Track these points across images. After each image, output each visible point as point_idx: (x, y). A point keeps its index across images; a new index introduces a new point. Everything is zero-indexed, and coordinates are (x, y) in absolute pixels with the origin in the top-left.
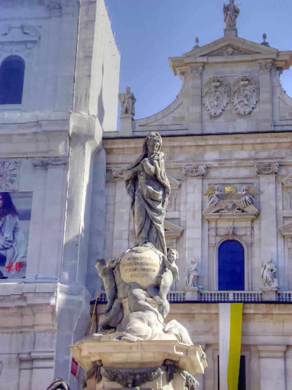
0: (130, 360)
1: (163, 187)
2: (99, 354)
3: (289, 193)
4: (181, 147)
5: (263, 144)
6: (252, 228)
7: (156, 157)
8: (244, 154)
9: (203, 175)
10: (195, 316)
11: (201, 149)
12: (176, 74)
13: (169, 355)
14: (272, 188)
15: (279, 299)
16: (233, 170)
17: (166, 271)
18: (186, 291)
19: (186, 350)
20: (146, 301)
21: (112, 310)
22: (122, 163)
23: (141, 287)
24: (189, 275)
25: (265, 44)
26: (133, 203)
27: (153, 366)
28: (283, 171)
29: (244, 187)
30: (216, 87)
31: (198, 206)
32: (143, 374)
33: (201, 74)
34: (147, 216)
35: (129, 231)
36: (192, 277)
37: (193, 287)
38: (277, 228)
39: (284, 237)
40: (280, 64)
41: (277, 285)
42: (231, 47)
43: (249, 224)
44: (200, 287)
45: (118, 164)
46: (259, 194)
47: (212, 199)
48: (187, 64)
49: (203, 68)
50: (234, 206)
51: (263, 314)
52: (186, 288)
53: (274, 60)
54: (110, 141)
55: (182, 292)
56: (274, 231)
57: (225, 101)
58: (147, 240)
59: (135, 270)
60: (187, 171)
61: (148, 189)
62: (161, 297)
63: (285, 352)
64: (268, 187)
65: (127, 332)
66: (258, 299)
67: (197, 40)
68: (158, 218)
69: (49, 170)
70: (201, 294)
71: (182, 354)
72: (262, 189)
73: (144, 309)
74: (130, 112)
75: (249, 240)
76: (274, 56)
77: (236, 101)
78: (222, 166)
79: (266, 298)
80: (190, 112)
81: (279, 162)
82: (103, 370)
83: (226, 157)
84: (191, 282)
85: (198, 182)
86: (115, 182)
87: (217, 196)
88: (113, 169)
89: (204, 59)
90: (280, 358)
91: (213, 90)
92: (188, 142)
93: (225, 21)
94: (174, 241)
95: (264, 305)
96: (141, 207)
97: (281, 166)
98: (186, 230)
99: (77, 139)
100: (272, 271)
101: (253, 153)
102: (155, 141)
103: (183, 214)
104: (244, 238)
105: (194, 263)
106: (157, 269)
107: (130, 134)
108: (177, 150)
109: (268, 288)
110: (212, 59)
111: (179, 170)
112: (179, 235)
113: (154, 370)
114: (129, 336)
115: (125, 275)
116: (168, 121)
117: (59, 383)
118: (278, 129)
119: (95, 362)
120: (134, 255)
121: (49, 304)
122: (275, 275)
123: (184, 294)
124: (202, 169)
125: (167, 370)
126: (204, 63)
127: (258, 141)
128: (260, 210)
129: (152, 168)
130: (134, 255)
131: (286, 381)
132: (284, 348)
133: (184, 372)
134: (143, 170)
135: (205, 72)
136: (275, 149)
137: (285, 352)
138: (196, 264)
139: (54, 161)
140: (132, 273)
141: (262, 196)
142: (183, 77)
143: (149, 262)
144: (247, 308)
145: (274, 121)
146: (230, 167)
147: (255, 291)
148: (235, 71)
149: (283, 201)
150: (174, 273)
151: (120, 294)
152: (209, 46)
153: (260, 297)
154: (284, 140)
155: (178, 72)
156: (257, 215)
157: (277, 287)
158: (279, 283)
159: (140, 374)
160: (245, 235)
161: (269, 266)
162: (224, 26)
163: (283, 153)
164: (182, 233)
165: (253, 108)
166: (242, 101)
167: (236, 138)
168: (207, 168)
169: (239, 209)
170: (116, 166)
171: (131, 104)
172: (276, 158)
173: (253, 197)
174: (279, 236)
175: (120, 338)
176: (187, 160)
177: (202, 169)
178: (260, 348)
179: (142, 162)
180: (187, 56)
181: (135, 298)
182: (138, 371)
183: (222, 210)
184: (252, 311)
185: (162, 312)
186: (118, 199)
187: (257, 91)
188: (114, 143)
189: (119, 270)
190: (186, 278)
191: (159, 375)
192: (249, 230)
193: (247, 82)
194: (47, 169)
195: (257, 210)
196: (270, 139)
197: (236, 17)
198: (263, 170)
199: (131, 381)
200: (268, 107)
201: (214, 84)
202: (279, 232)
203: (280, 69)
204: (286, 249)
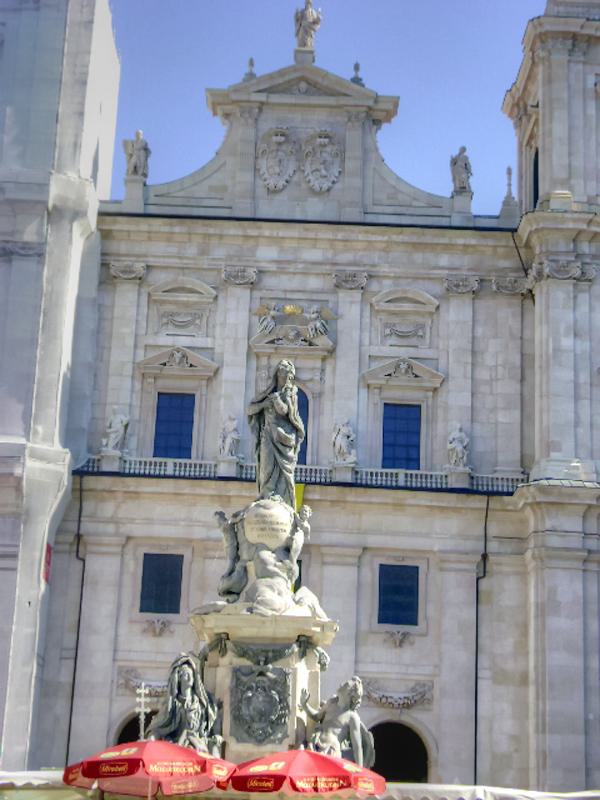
0: (261, 635)
1: (295, 429)
2: (227, 627)
3: (381, 320)
4: (221, 236)
5: (347, 241)
6: (323, 370)
7: (289, 393)
8: (315, 255)
9: (252, 283)
10: (232, 499)
11: (251, 242)
12: (215, 114)
13: (304, 630)
14: (355, 310)
15: (356, 479)
16: (298, 277)
17: (297, 531)
18: (219, 462)
19: (323, 626)
20: (275, 565)
21: (235, 573)
22: (127, 255)
23: (269, 549)
24: (225, 438)
25: (357, 80)
26: (258, 444)
27: (287, 642)
28: (374, 286)
29: (315, 307)
30: (280, 144)
31: (242, 332)
32: (277, 651)
33: (256, 120)
34: (276, 464)
35: (134, 363)
36: (229, 441)
37: (230, 457)
38: (359, 372)
40: (378, 115)
41: (355, 459)
42: (303, 82)
43: (318, 364)
44: (241, 455)
45: (119, 255)
46: (337, 319)
47: (265, 323)
48: (234, 102)
49: (260, 110)
50: (298, 335)
51: (332, 501)
52: (220, 458)
53: (370, 108)
54: (108, 218)
55: (213, 463)
56: (355, 376)
57: (292, 166)
58: (276, 491)
59: (262, 529)
60: (229, 276)
61: (279, 433)
62: (292, 561)
63: (360, 557)
64: (350, 309)
65: (258, 603)
66: (325, 478)
67: (251, 63)
68: (288, 466)
69: (14, 263)
70: (242, 467)
71: (318, 629)
72: (340, 311)
73: (272, 575)
74: (140, 172)
75: (317, 388)
76: (371, 103)
77: (308, 169)
78: (282, 271)
79: (338, 477)
80: (236, 187)
81: (367, 271)
82: (229, 644)
83: (289, 257)
86: (114, 285)
87: (273, 317)
88: (112, 263)
89: (262, 97)
90: (352, 565)
91: (274, 147)
92: (232, 229)
93: (297, 35)
94: (204, 383)
95: (335, 488)
96: (270, 453)
97: (370, 277)
98: (222, 366)
99: (59, 215)
100: (348, 437)
101: (330, 254)
102: (288, 372)
103: (219, 341)
104: (310, 385)
105: (234, 419)
106: (289, 528)
107: (141, 210)
108: (214, 241)
109: (340, 462)
110: (275, 98)
111: (215, 273)
112: (212, 374)
113: (289, 646)
114: (262, 609)
115: (251, 534)
116: (201, 191)
117: (184, 659)
118: (370, 219)
119: (219, 634)
120: (262, 510)
121: (12, 474)
122: (352, 444)
123: (216, 466)
124: (251, 273)
125: (300, 646)
126: (262, 103)
128: (335, 343)
129: (285, 407)
130: (262, 510)
131: (358, 599)
132: (359, 551)
133: (319, 648)
134: (273, 406)
135: (263, 116)
136: (365, 250)
137: (360, 557)
138: (235, 423)
139: (23, 248)
140: (260, 532)
141: (339, 321)
142: (226, 121)
143: (280, 521)
144: (309, 492)
145: (364, 206)
146: (294, 274)
147: (321, 465)
148: (311, 120)
149: (370, 332)
150: (306, 533)
151: (244, 555)
152: (271, 76)
153: (328, 476)
154: (380, 238)
155: (220, 112)
156: (332, 352)
157: (355, 463)
158: (357, 456)
159: (273, 651)
160: (311, 380)
161: (344, 430)
163: (375, 257)
164: (217, 372)
165: (334, 182)
166: (317, 170)
167: (307, 230)
168: (261, 272)
169: (305, 340)
170: (117, 258)
171: (142, 159)
172: (365, 265)
173: (327, 322)
174: (361, 384)
175: (250, 610)
176: (230, 257)
177: (251, 273)
178: (324, 550)
179: (272, 396)
180: (236, 89)
181: (264, 563)
182: (271, 648)
183: (279, 339)
184: (317, 497)
185: (290, 578)
186: (117, 311)
187: (341, 155)
188: (115, 223)
189: (243, 527)
190: (220, 441)
191: (293, 652)
193: (326, 140)
194: (10, 261)
195: (331, 343)
196: (360, 234)
198: (345, 281)
199: (263, 659)
200: (357, 182)
201: (275, 139)
202: (362, 378)
203: (377, 123)
204: (371, 406)
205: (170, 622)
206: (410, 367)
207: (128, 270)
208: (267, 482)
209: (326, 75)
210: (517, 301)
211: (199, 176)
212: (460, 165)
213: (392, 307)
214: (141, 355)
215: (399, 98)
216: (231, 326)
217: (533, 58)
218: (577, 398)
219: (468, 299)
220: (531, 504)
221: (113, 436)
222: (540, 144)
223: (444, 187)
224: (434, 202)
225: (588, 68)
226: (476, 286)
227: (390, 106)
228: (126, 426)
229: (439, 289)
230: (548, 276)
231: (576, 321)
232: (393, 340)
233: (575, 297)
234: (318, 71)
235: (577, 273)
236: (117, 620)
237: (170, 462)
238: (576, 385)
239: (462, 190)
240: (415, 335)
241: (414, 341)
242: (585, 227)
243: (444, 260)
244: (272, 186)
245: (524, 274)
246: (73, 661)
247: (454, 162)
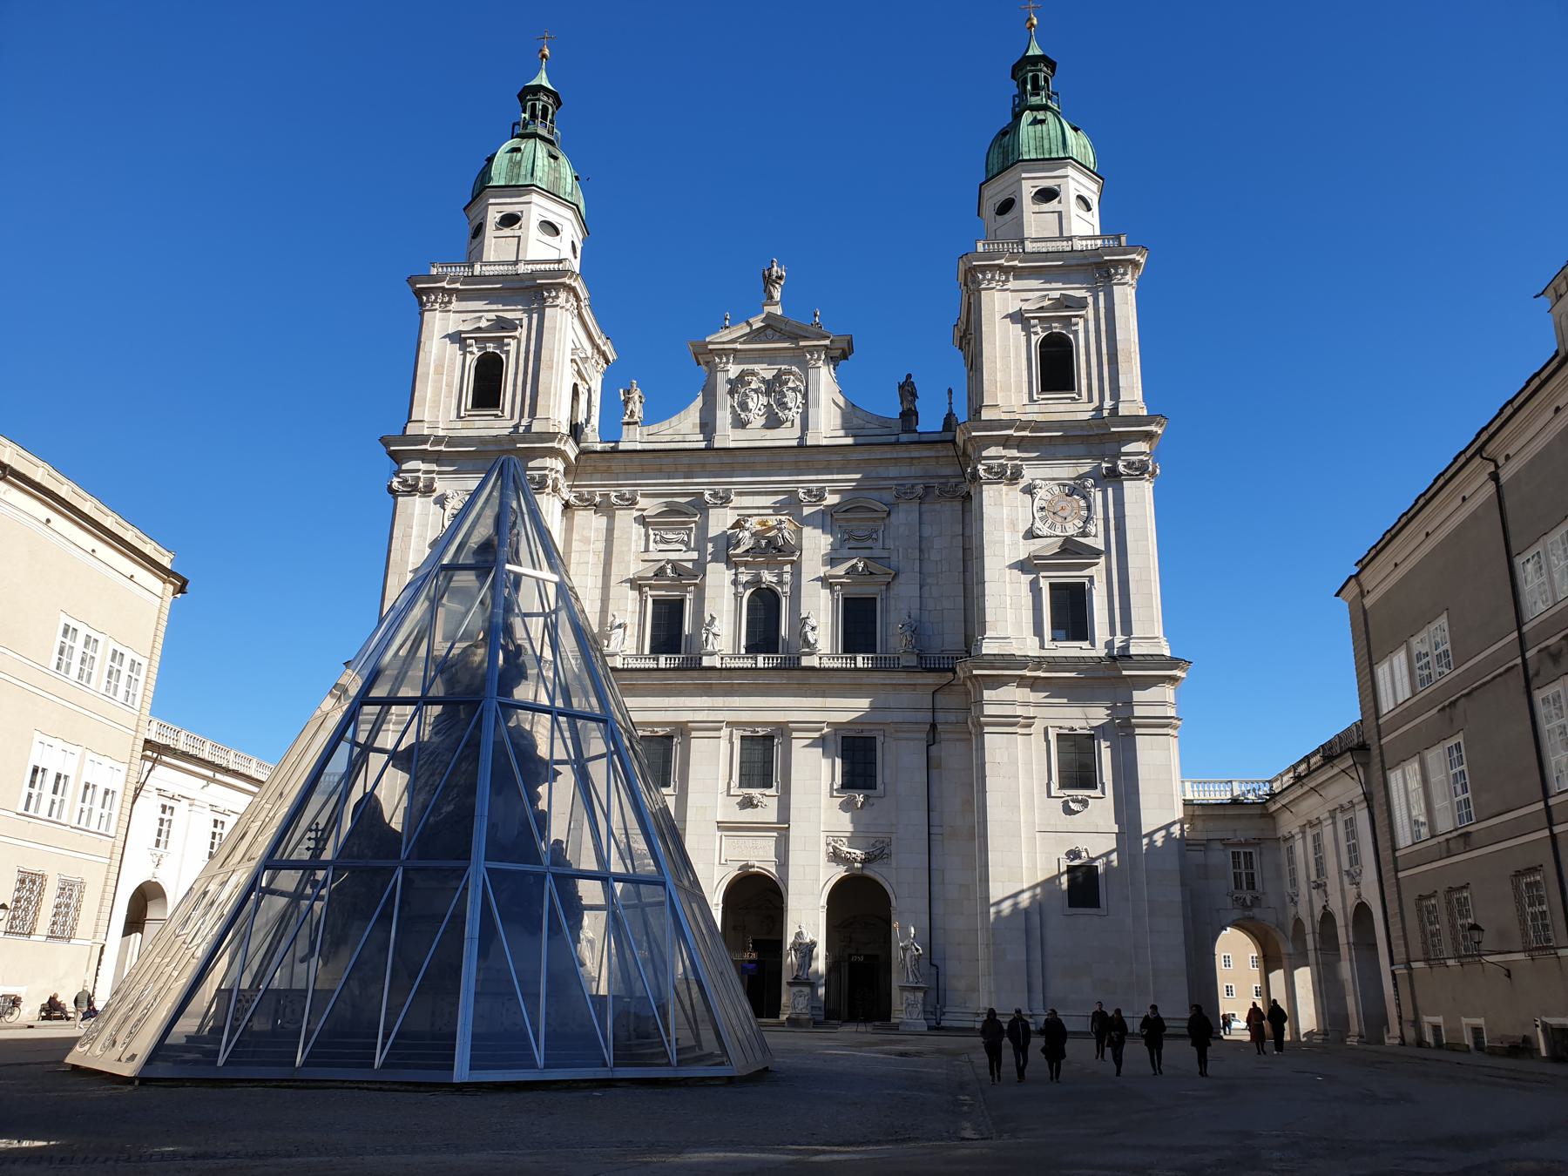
4: (704, 465)
207: (621, 497)
212: (908, 390)
213: (849, 515)
219: (915, 505)
224: (884, 422)
226: (919, 490)
229: (888, 496)
232: (853, 544)
240: (870, 537)
241: (869, 543)
243: (893, 471)
247: (901, 387)
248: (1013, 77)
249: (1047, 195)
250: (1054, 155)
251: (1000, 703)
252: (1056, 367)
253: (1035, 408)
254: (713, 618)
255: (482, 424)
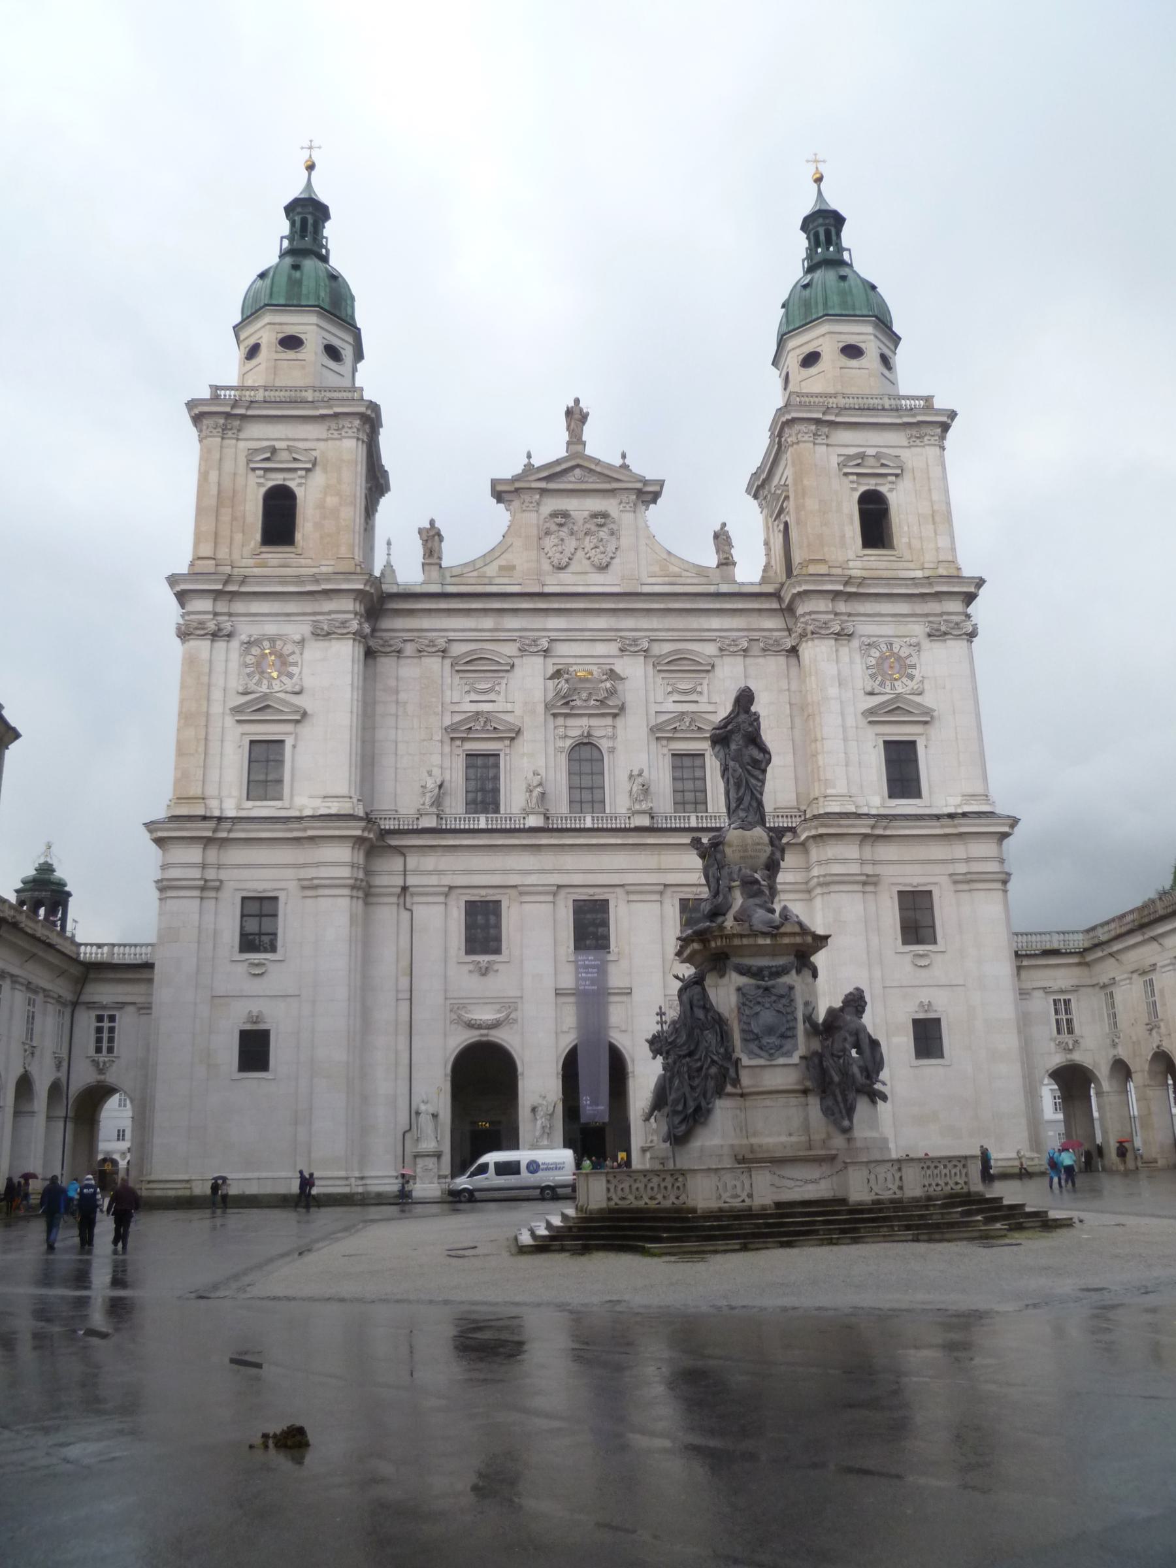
25: (625, 467)
39: (658, 738)
56: (644, 731)
64: (634, 670)
67: (529, 456)
76: (639, 485)
84: (534, 801)
85: (540, 660)
89: (543, 485)
109: (637, 807)
116: (491, 570)
124: (544, 644)
127: (621, 606)
161: (640, 780)
162: (566, 436)
165: (612, 558)
180: (516, 479)
192: (610, 730)
197: (584, 423)
198: (628, 648)
204: (661, 757)
205: (495, 962)
206: (692, 721)
207: (432, 643)
208: (738, 807)
209: (598, 462)
210: (782, 660)
211: (488, 557)
212: (722, 539)
214: (447, 722)
215: (664, 481)
216: (526, 689)
217: (780, 443)
218: (845, 740)
219: (740, 660)
220: (814, 837)
221: (428, 795)
222: (791, 519)
223: (710, 559)
225: (830, 449)
227: (656, 488)
228: (440, 786)
230: (813, 633)
231: (839, 674)
232: (677, 697)
233: (837, 651)
234: (591, 459)
235: (837, 629)
236: (446, 962)
237: (483, 818)
238: (844, 727)
239: (726, 562)
242: (840, 588)
243: (715, 622)
244: (556, 562)
245: (786, 633)
246: (408, 1002)
247: (716, 536)
248: (804, 227)
249: (852, 351)
250: (858, 313)
251: (845, 861)
252: (875, 522)
253: (859, 564)
254: (536, 774)
255: (275, 562)
